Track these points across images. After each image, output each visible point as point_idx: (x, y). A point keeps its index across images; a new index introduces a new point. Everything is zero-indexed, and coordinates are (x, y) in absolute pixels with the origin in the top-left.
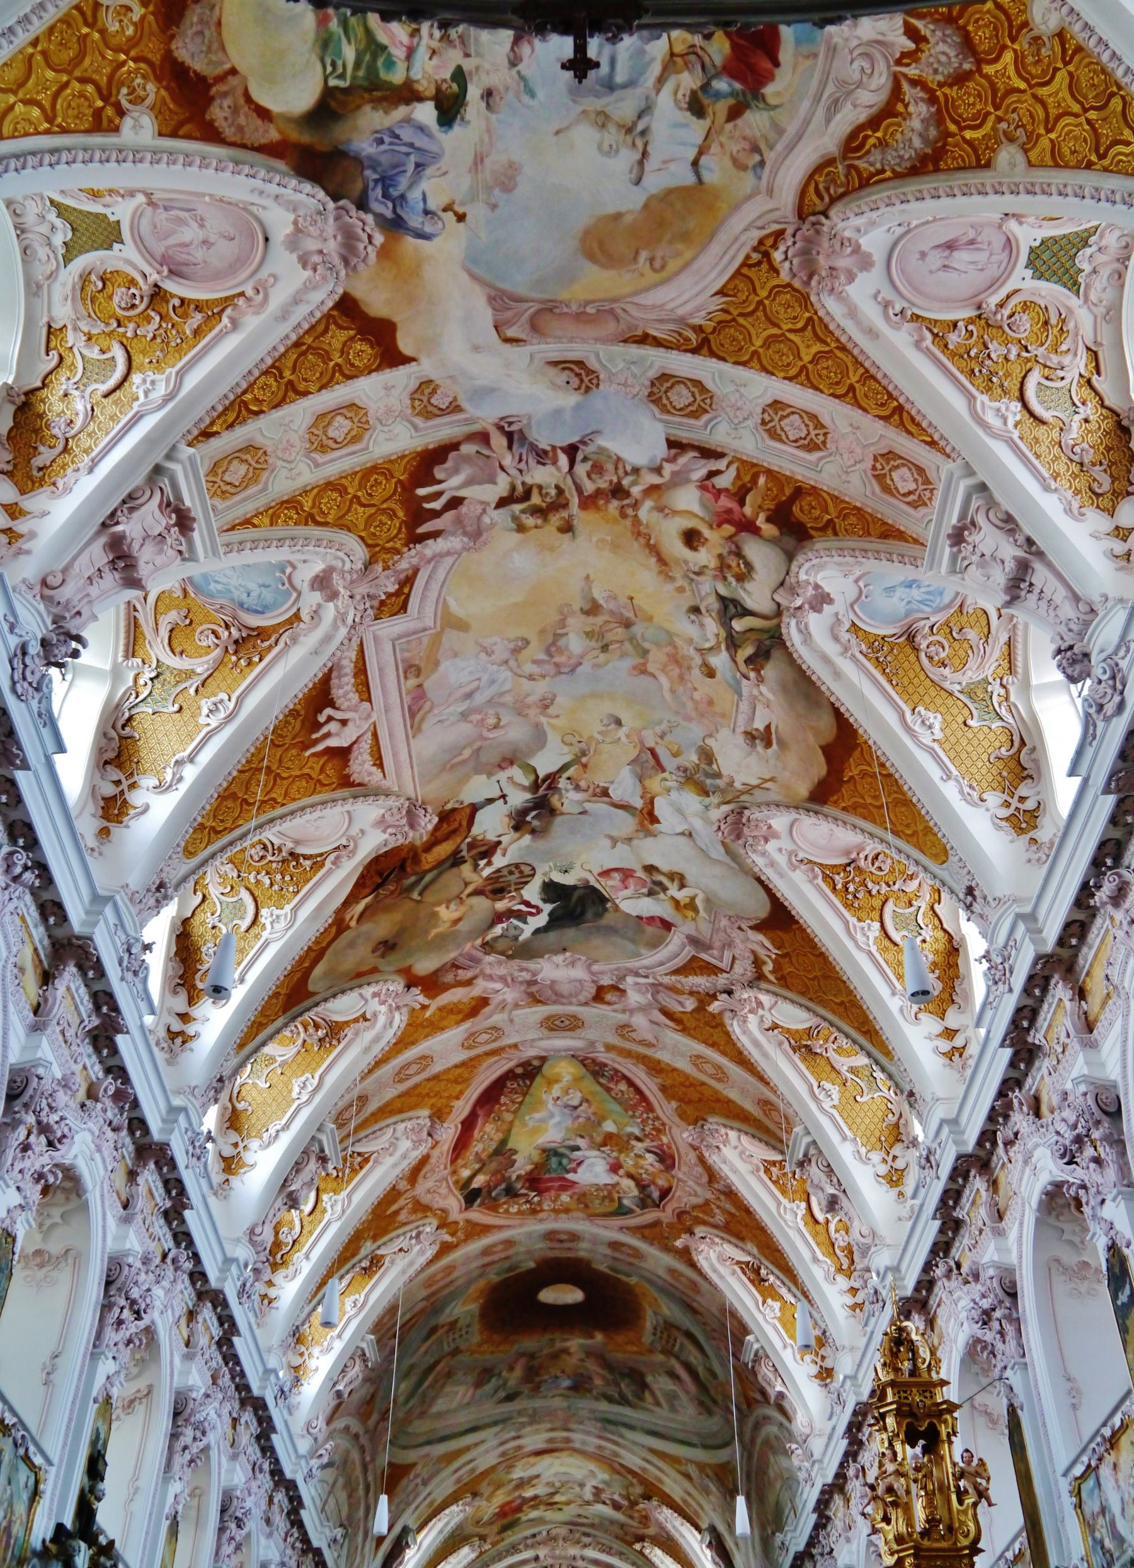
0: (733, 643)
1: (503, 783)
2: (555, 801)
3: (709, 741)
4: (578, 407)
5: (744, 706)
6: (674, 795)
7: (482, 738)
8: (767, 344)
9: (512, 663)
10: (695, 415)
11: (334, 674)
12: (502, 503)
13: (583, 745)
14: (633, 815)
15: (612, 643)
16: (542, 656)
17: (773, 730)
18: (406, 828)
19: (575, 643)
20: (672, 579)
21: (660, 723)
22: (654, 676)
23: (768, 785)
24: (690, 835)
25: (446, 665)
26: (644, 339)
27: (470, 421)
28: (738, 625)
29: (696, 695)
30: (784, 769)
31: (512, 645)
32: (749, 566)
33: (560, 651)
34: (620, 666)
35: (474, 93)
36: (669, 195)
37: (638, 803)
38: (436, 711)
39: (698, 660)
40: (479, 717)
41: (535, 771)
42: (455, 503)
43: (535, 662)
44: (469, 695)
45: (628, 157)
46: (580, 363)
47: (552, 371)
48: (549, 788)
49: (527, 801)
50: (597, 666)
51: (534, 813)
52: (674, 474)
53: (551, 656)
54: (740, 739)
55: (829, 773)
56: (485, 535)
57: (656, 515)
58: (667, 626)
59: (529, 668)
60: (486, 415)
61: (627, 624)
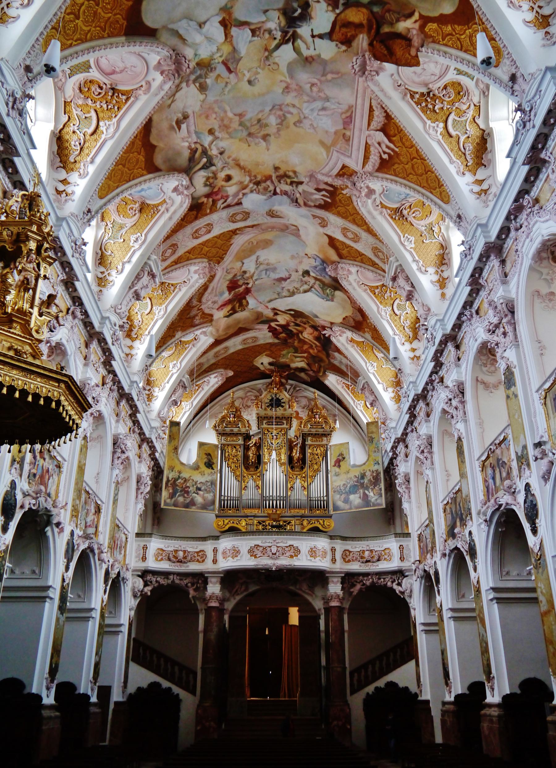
0: (205, 152)
1: (312, 48)
2: (283, 23)
3: (202, 97)
4: (273, 206)
5: (192, 128)
7: (321, 81)
8: (216, 243)
9: (302, 117)
10: (234, 214)
11: (376, 168)
12: (301, 183)
13: (268, 63)
14: (236, 20)
15: (256, 125)
16: (288, 116)
17: (177, 130)
18: (368, 62)
19: (273, 120)
20: (234, 160)
21: (229, 92)
22: (235, 115)
23: (170, 101)
24: (200, 26)
25: (333, 130)
26: (253, 226)
27: (310, 211)
28: (205, 160)
29: (214, 116)
30: (167, 117)
31: (302, 125)
32: (206, 185)
33: (279, 117)
34: (251, 115)
35: (301, 273)
36: (249, 256)
37: (234, 31)
38: (340, 110)
39: (217, 134)
40: (320, 94)
42: (318, 190)
43: (292, 114)
44: (324, 109)
45: (261, 259)
46: (272, 217)
47: (281, 215)
49: (300, 27)
50: (262, 111)
51: (296, 14)
52: (238, 195)
53: (284, 115)
55: (149, 141)
56: (309, 174)
57: (243, 180)
58: (232, 140)
59: (294, 110)
60: (303, 210)
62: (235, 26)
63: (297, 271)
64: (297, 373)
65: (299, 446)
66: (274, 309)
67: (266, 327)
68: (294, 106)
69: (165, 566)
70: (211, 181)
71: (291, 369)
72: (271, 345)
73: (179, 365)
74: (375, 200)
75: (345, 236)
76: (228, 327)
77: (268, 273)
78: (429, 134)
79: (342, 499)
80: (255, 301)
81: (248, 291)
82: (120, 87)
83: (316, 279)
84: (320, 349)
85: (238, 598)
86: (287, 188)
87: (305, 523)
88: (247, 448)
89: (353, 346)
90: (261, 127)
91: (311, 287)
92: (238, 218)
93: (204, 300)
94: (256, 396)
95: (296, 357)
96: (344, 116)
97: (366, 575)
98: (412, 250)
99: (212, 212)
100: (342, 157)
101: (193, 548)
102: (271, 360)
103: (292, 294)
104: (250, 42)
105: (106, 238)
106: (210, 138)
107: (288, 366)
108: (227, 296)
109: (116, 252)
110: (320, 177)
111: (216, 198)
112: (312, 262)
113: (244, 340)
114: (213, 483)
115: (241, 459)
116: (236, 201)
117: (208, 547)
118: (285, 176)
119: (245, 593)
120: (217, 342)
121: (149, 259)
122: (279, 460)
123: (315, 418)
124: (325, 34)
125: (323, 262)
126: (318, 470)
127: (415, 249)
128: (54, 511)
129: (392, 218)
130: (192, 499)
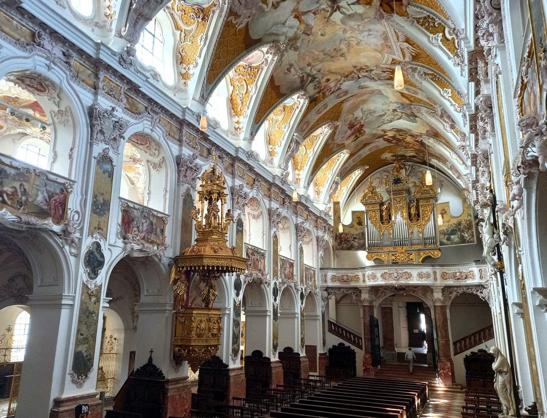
0: (309, 75)
1: (350, 10)
3: (297, 53)
5: (297, 68)
6: (295, 29)
7: (362, 23)
9: (359, 40)
12: (373, 70)
16: (351, 42)
17: (289, 73)
19: (343, 46)
23: (280, 63)
24: (284, 24)
25: (379, 44)
26: (352, 96)
28: (310, 78)
29: (308, 57)
32: (315, 89)
37: (303, 18)
39: (312, 64)
41: (341, 13)
42: (384, 72)
43: (353, 41)
44: (370, 35)
45: (365, 109)
48: (334, 7)
49: (340, 2)
50: (334, 45)
53: (348, 42)
54: (293, 62)
55: (275, 85)
58: (322, 63)
60: (379, 82)
61: (332, 57)
62: (303, 15)
63: (389, 110)
64: (412, 158)
65: (414, 206)
66: (383, 130)
67: (382, 139)
68: (352, 37)
69: (337, 284)
70: (318, 85)
71: (407, 157)
72: (389, 147)
73: (331, 172)
74: (419, 72)
75: (409, 92)
76: (357, 146)
77: (371, 114)
78: (432, 44)
79: (446, 238)
80: (369, 129)
81: (362, 126)
82: (253, 65)
83: (402, 112)
84: (420, 146)
85: (381, 300)
86: (365, 74)
87: (422, 254)
88: (381, 211)
89: (439, 144)
90: (337, 51)
91: (401, 117)
92: (341, 95)
93: (335, 138)
94: (387, 176)
95: (407, 151)
96: (383, 37)
97: (460, 287)
98: (450, 98)
99: (324, 98)
100: (390, 55)
101: (352, 274)
102: (392, 154)
103: (391, 121)
104: (314, 18)
105: (270, 129)
106: (309, 68)
107: (405, 156)
108: (349, 132)
109: (276, 136)
110: (382, 66)
111: (324, 92)
112: (396, 105)
113: (370, 149)
114: (363, 234)
115: (378, 218)
116: (337, 88)
117: (360, 274)
118: (361, 69)
119: (385, 297)
120: (351, 155)
121: (293, 135)
122: (402, 216)
123: (424, 187)
124: (355, 2)
125: (402, 104)
126: (429, 220)
127: (452, 97)
128: (263, 278)
129: (433, 80)
130: (352, 245)
